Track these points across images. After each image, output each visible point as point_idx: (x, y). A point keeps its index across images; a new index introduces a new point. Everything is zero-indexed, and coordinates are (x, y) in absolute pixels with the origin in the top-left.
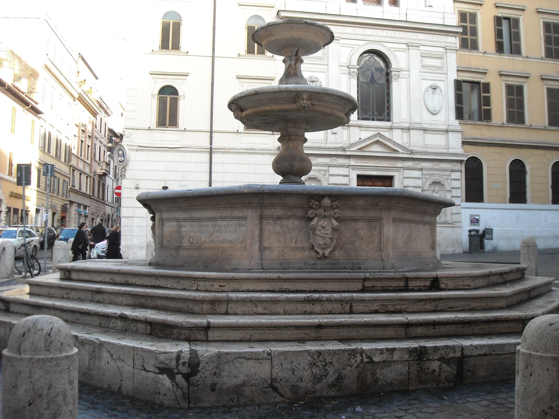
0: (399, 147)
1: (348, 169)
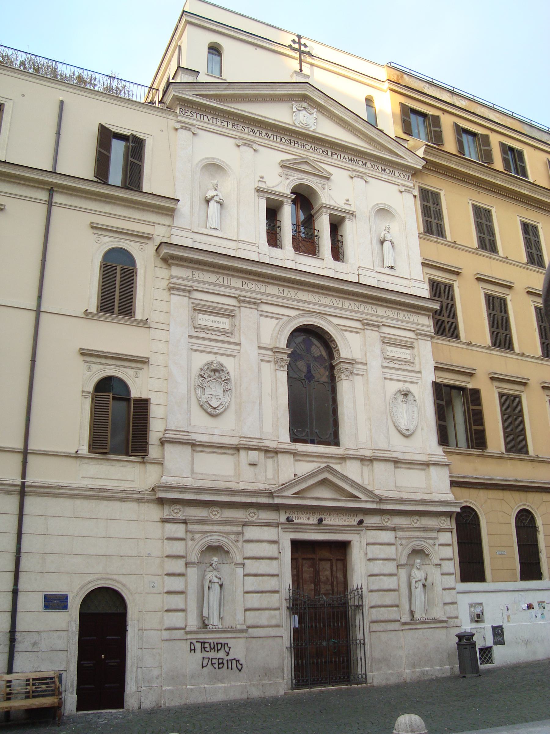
0: (360, 491)
1: (277, 529)
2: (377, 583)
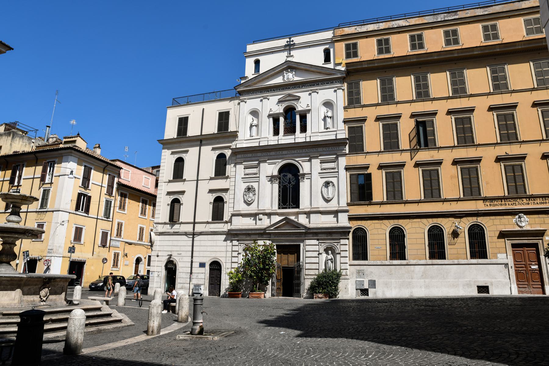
2: (308, 260)
